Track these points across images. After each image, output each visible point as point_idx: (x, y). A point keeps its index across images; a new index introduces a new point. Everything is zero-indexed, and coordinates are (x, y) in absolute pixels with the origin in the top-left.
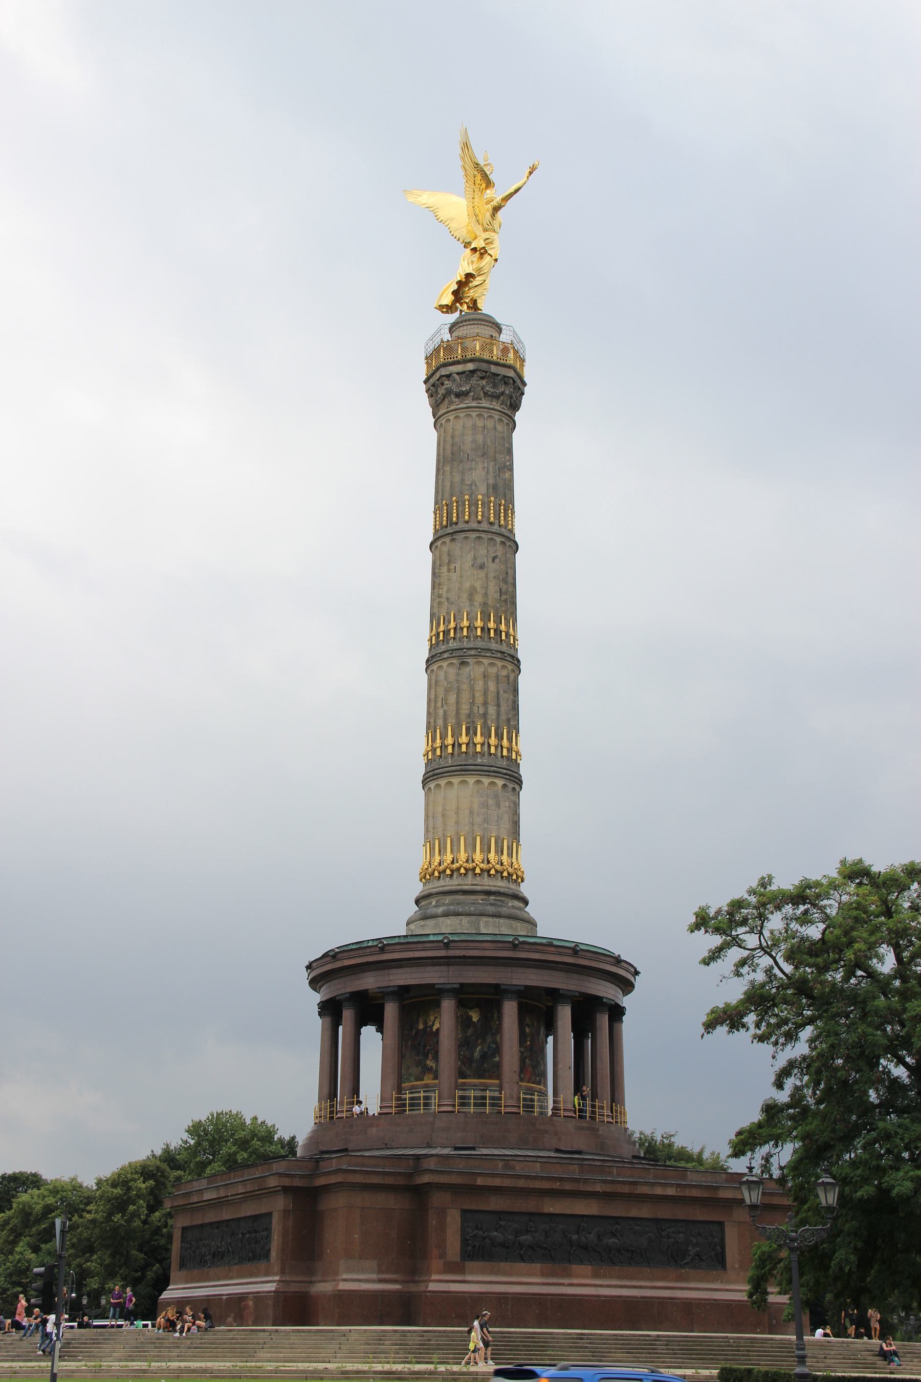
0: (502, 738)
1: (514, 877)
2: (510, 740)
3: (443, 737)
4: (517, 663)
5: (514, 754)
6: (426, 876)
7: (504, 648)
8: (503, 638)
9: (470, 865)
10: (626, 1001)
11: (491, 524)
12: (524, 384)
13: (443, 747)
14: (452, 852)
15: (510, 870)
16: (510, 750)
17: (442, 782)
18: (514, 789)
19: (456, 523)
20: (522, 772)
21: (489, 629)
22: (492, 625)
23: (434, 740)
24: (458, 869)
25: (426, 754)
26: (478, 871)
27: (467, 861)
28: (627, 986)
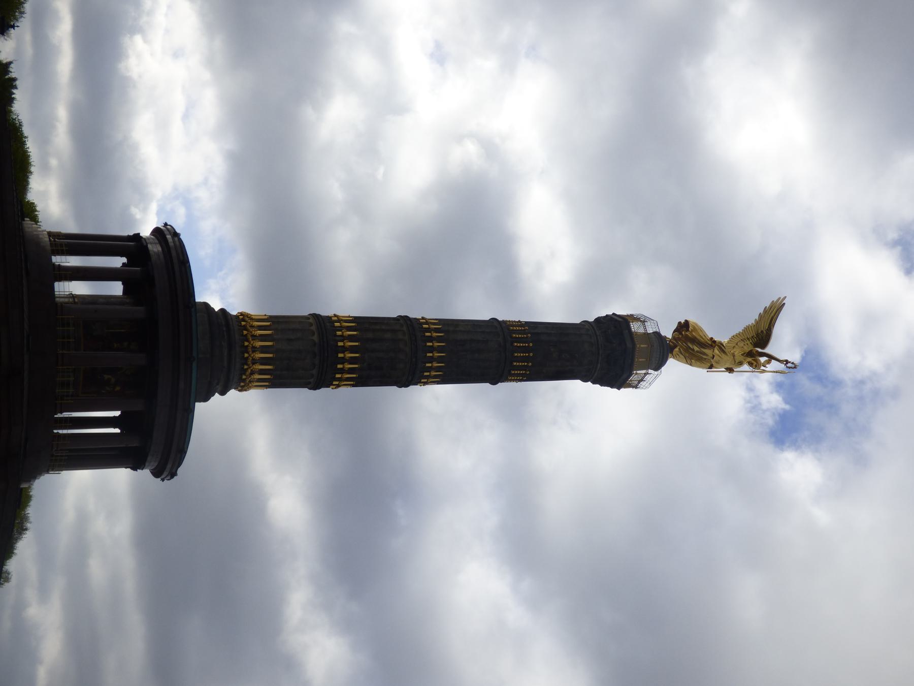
1: (242, 384)
11: (512, 363)
14: (261, 335)
16: (340, 379)
18: (310, 383)
19: (511, 337)
21: (431, 362)
23: (346, 321)
25: (335, 316)
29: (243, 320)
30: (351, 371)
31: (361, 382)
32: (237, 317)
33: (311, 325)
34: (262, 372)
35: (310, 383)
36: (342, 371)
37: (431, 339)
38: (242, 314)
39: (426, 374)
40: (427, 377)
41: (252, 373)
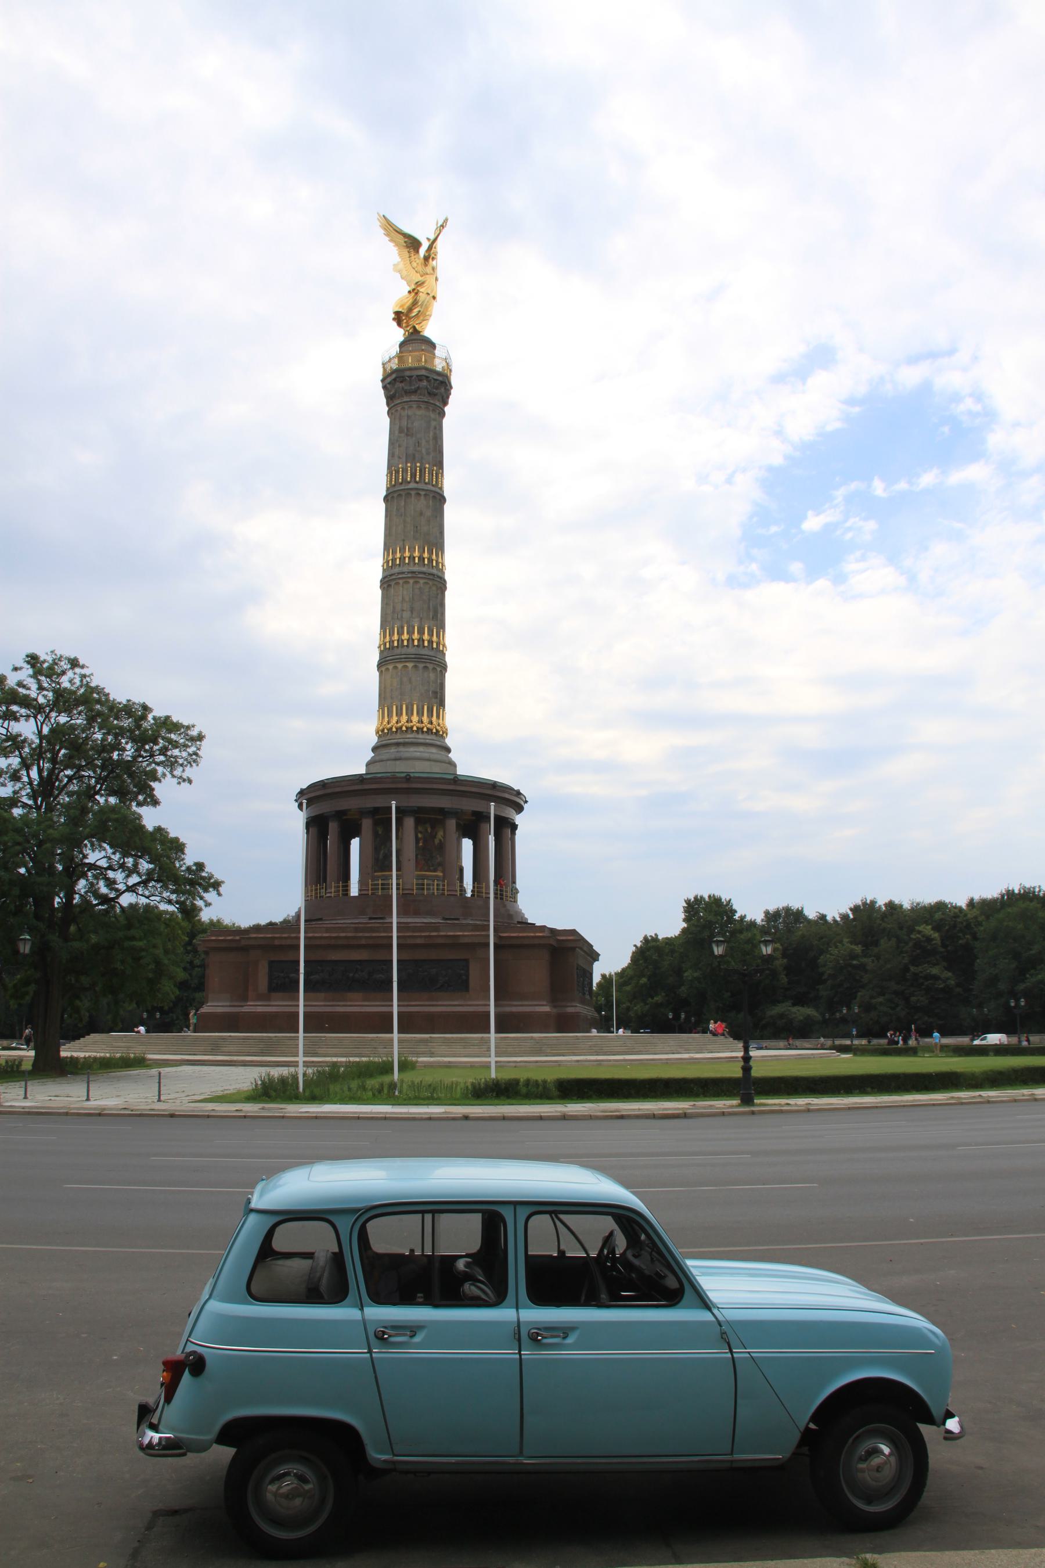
2: (438, 636)
3: (391, 634)
6: (381, 733)
7: (434, 571)
9: (410, 725)
10: (519, 819)
13: (391, 642)
16: (438, 644)
17: (391, 667)
22: (426, 555)
23: (385, 637)
24: (401, 728)
25: (379, 647)
26: (415, 728)
28: (519, 809)
30: (431, 634)
31: (441, 626)
32: (380, 737)
37: (403, 558)
38: (377, 732)
41: (431, 723)
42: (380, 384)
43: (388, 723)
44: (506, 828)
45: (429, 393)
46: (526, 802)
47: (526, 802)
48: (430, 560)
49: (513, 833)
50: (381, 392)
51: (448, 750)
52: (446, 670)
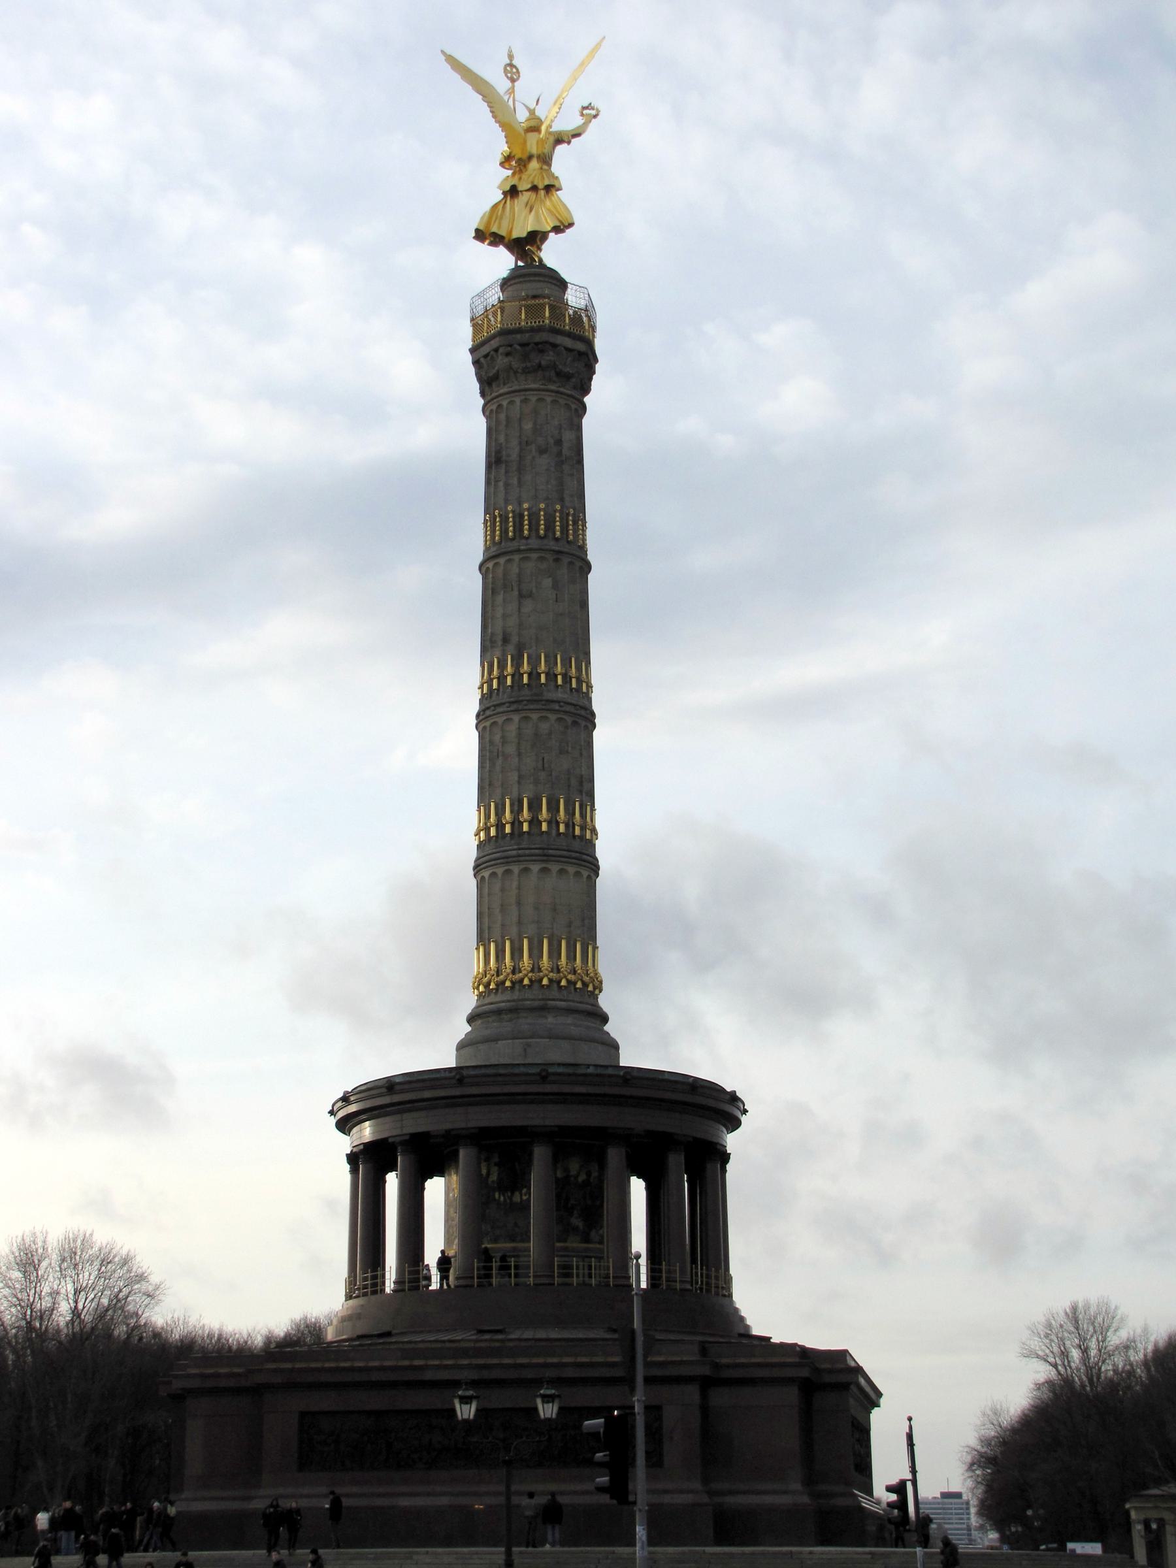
0: (574, 814)
1: (590, 988)
2: (583, 815)
4: (593, 714)
5: (588, 832)
8: (574, 685)
10: (732, 1141)
11: (557, 540)
12: (596, 361)
14: (512, 958)
15: (586, 979)
16: (583, 828)
19: (513, 539)
20: (598, 854)
23: (488, 817)
27: (532, 971)
29: (487, 985)
31: (587, 795)
32: (480, 995)
33: (494, 874)
34: (571, 957)
35: (589, 877)
36: (570, 825)
37: (517, 676)
39: (574, 685)
40: (579, 681)
41: (574, 972)
42: (468, 358)
43: (498, 973)
44: (709, 1162)
45: (558, 374)
46: (745, 1112)
47: (745, 1112)
48: (567, 678)
49: (724, 1171)
50: (472, 370)
51: (604, 1019)
52: (597, 875)
